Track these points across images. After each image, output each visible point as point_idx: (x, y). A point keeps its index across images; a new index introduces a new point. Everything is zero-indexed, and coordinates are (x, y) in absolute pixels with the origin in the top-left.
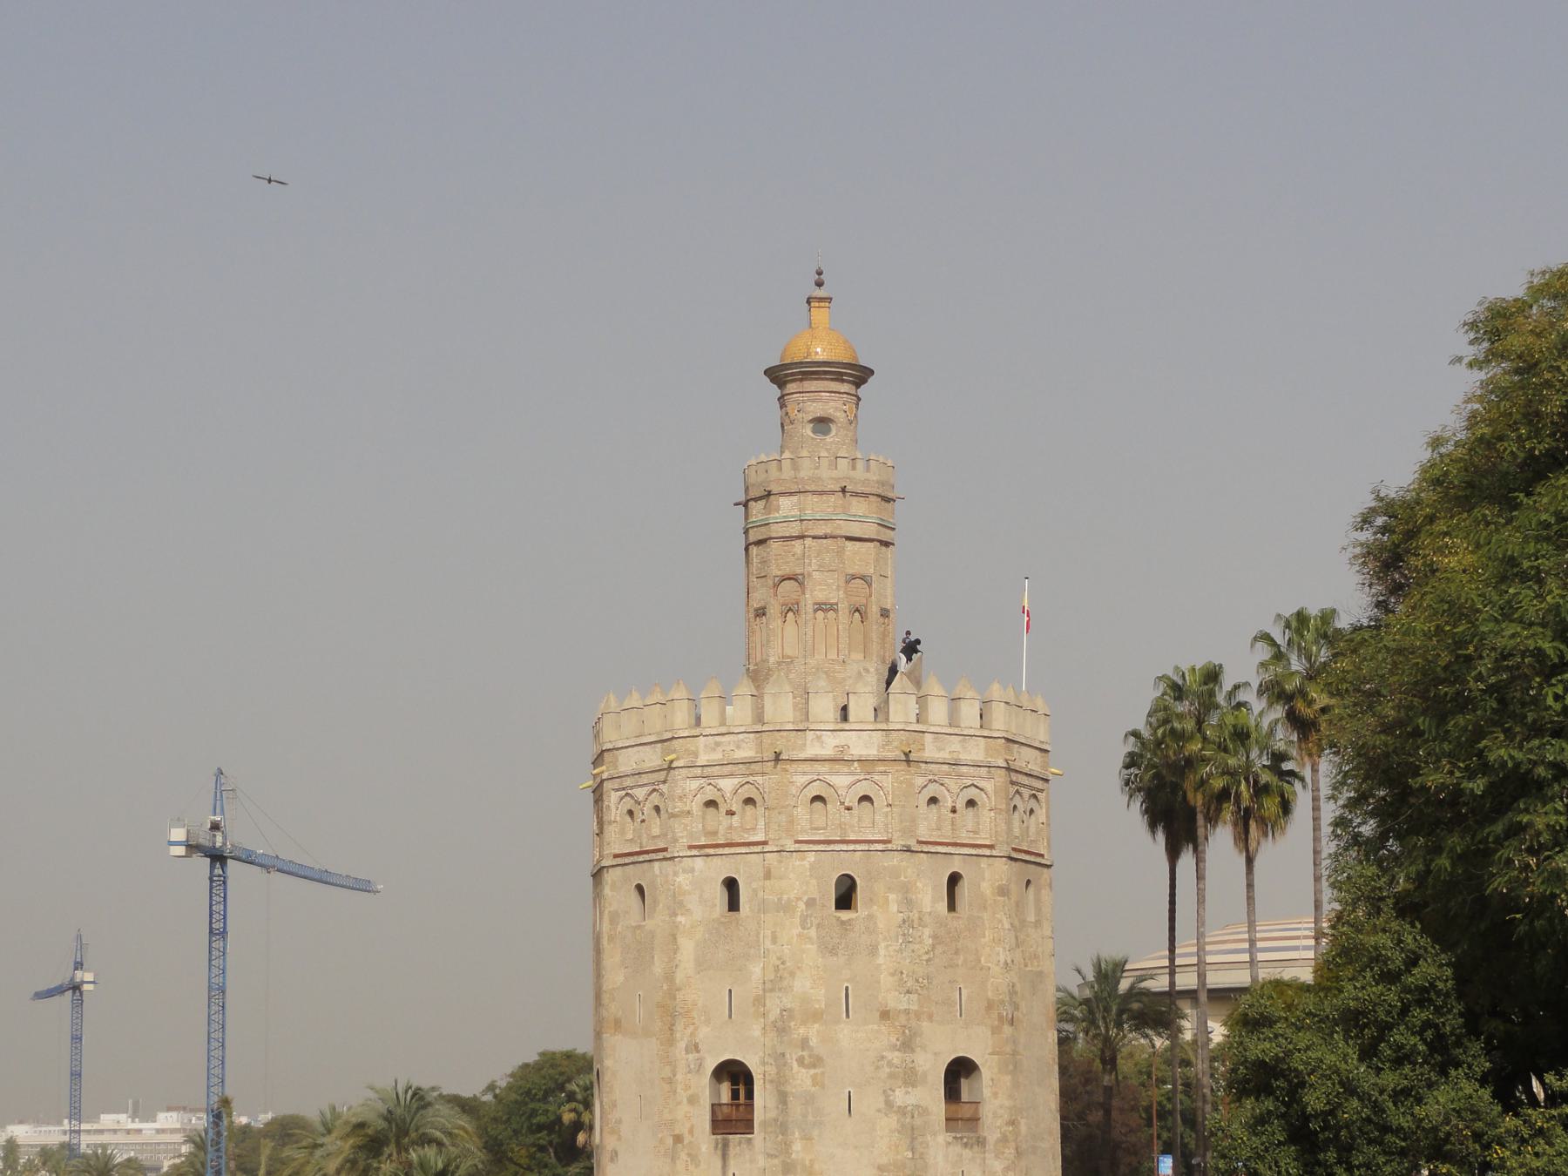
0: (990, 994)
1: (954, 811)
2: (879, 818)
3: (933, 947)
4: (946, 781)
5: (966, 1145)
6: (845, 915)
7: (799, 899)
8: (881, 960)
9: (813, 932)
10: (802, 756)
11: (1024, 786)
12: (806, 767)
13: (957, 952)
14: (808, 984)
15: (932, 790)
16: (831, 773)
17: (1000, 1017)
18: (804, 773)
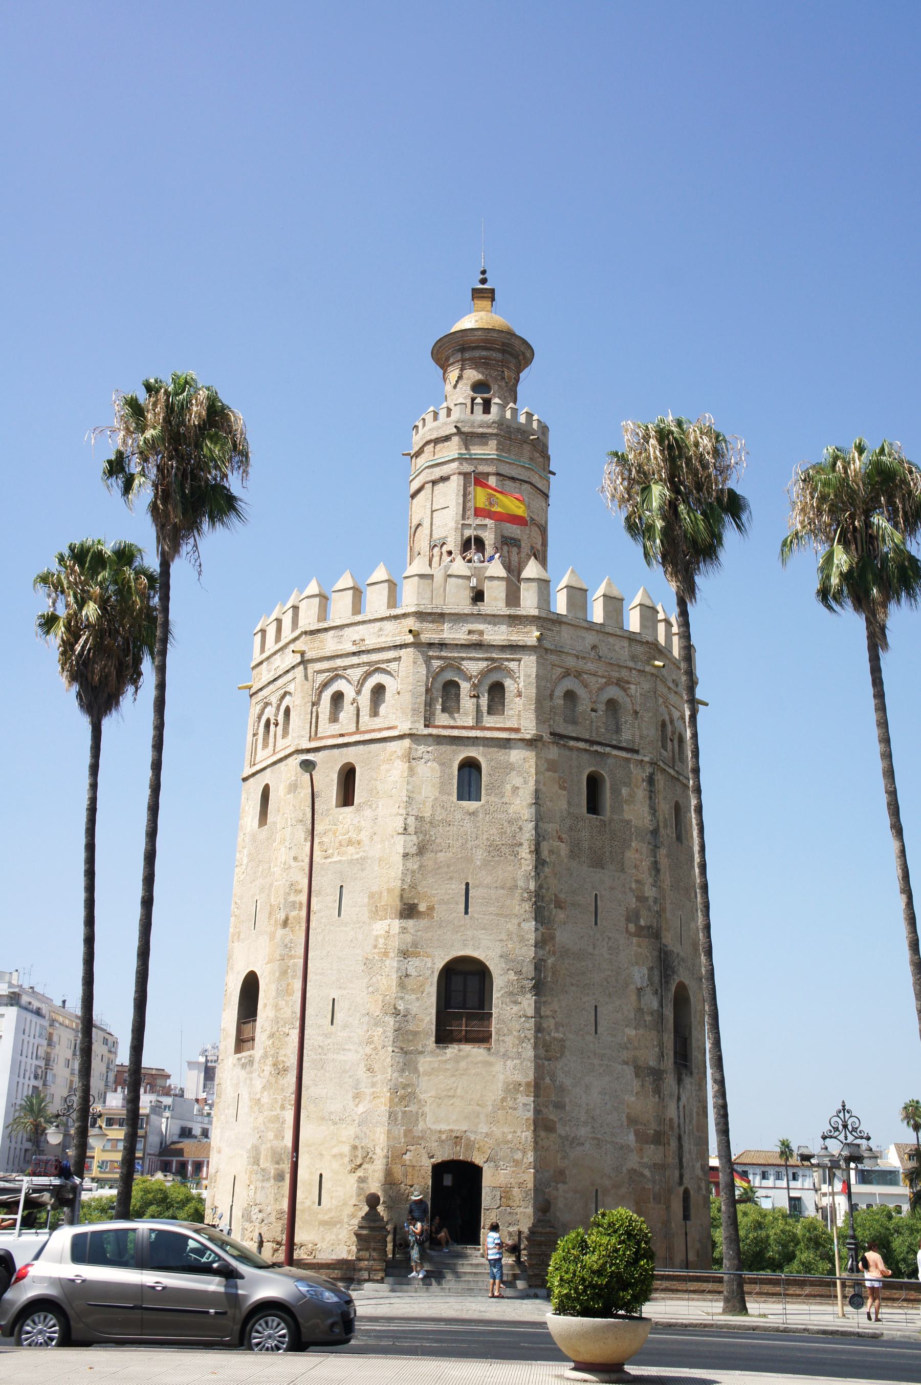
11: (352, 666)
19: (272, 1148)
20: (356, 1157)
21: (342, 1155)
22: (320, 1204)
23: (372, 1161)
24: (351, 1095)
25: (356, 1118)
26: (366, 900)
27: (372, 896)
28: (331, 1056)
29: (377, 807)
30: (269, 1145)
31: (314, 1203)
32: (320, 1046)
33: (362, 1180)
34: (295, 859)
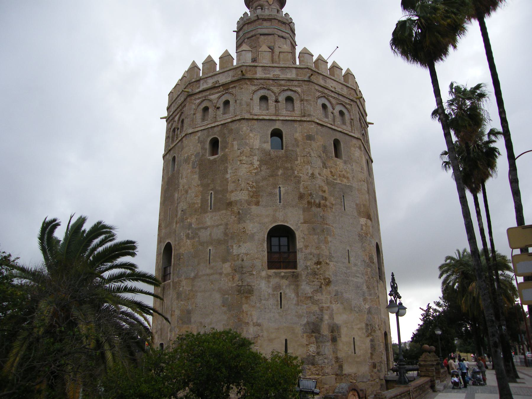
0: (301, 190)
1: (277, 101)
2: (231, 108)
3: (260, 166)
4: (271, 87)
5: (283, 277)
6: (212, 158)
7: (193, 154)
8: (228, 176)
9: (197, 170)
10: (197, 91)
12: (200, 95)
13: (278, 168)
14: (193, 195)
15: (262, 93)
16: (210, 95)
17: (309, 203)
18: (199, 98)
19: (328, 323)
20: (368, 329)
21: (362, 329)
22: (355, 353)
23: (375, 331)
24: (362, 299)
25: (366, 310)
26: (355, 206)
27: (357, 205)
28: (350, 278)
29: (352, 165)
30: (326, 322)
31: (352, 352)
32: (345, 273)
33: (372, 341)
34: (319, 174)
